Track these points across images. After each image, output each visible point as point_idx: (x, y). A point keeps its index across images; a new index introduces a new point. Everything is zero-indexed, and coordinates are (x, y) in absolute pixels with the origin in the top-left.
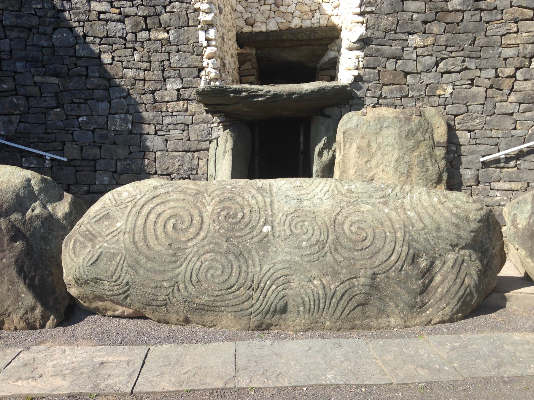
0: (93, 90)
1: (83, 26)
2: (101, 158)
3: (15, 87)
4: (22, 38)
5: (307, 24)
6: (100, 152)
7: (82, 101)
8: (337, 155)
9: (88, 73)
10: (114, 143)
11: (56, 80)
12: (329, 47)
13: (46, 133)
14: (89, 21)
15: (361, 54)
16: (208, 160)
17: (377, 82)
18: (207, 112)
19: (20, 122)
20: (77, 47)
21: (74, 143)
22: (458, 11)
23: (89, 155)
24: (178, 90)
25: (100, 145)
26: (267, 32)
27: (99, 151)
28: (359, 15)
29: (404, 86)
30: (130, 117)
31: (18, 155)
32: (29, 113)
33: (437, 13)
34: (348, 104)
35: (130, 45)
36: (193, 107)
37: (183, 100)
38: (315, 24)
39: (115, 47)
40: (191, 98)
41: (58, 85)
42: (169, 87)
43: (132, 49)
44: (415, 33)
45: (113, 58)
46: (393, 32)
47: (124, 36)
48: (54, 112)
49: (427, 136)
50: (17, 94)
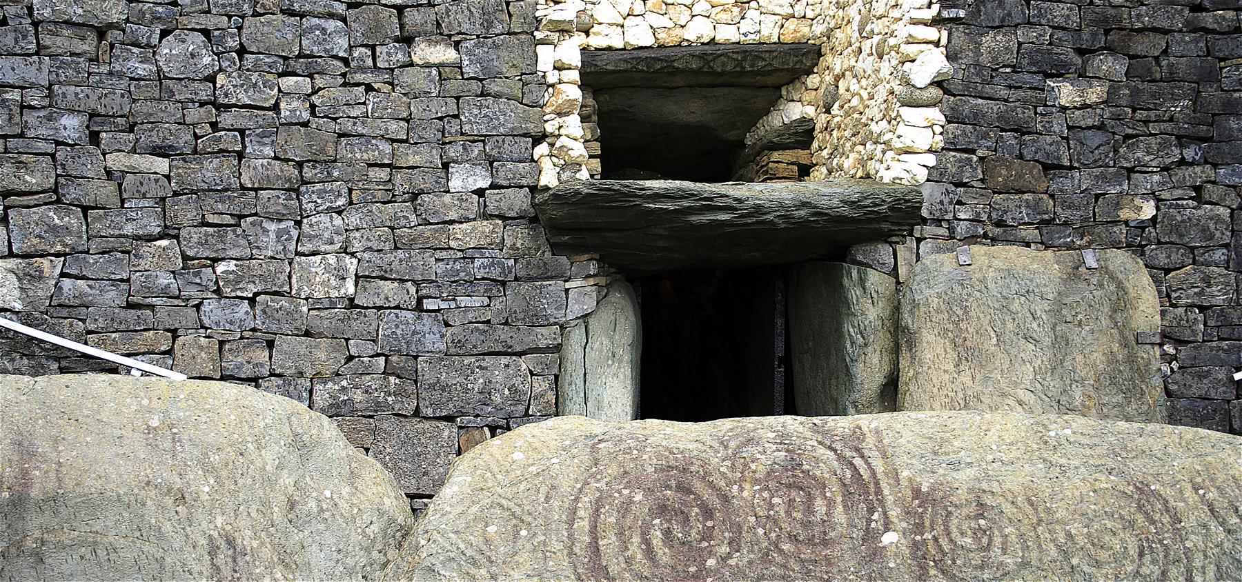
0: (256, 190)
1: (240, 28)
2: (271, 375)
3: (56, 183)
4: (78, 55)
5: (727, 34)
6: (270, 358)
7: (228, 220)
8: (903, 363)
9: (244, 147)
10: (307, 334)
11: (162, 165)
12: (784, 92)
13: (130, 306)
14: (256, 14)
15: (936, 115)
16: (556, 377)
17: (979, 184)
18: (556, 248)
19: (63, 275)
20: (221, 80)
21: (202, 331)
22: (1155, 30)
23: (240, 367)
24: (480, 192)
25: (270, 337)
26: (624, 49)
27: (267, 354)
28: (926, 25)
29: (1045, 197)
30: (351, 264)
31: (56, 366)
32: (88, 253)
33: (1107, 32)
34: (911, 235)
35: (359, 77)
36: (518, 236)
37: (492, 216)
38: (750, 37)
39: (319, 81)
40: (513, 214)
41: (168, 177)
42: (456, 183)
43: (362, 89)
44: (1061, 75)
45: (313, 107)
46: (1008, 70)
47: (341, 54)
48: (152, 250)
49: (1119, 317)
50: (58, 201)
